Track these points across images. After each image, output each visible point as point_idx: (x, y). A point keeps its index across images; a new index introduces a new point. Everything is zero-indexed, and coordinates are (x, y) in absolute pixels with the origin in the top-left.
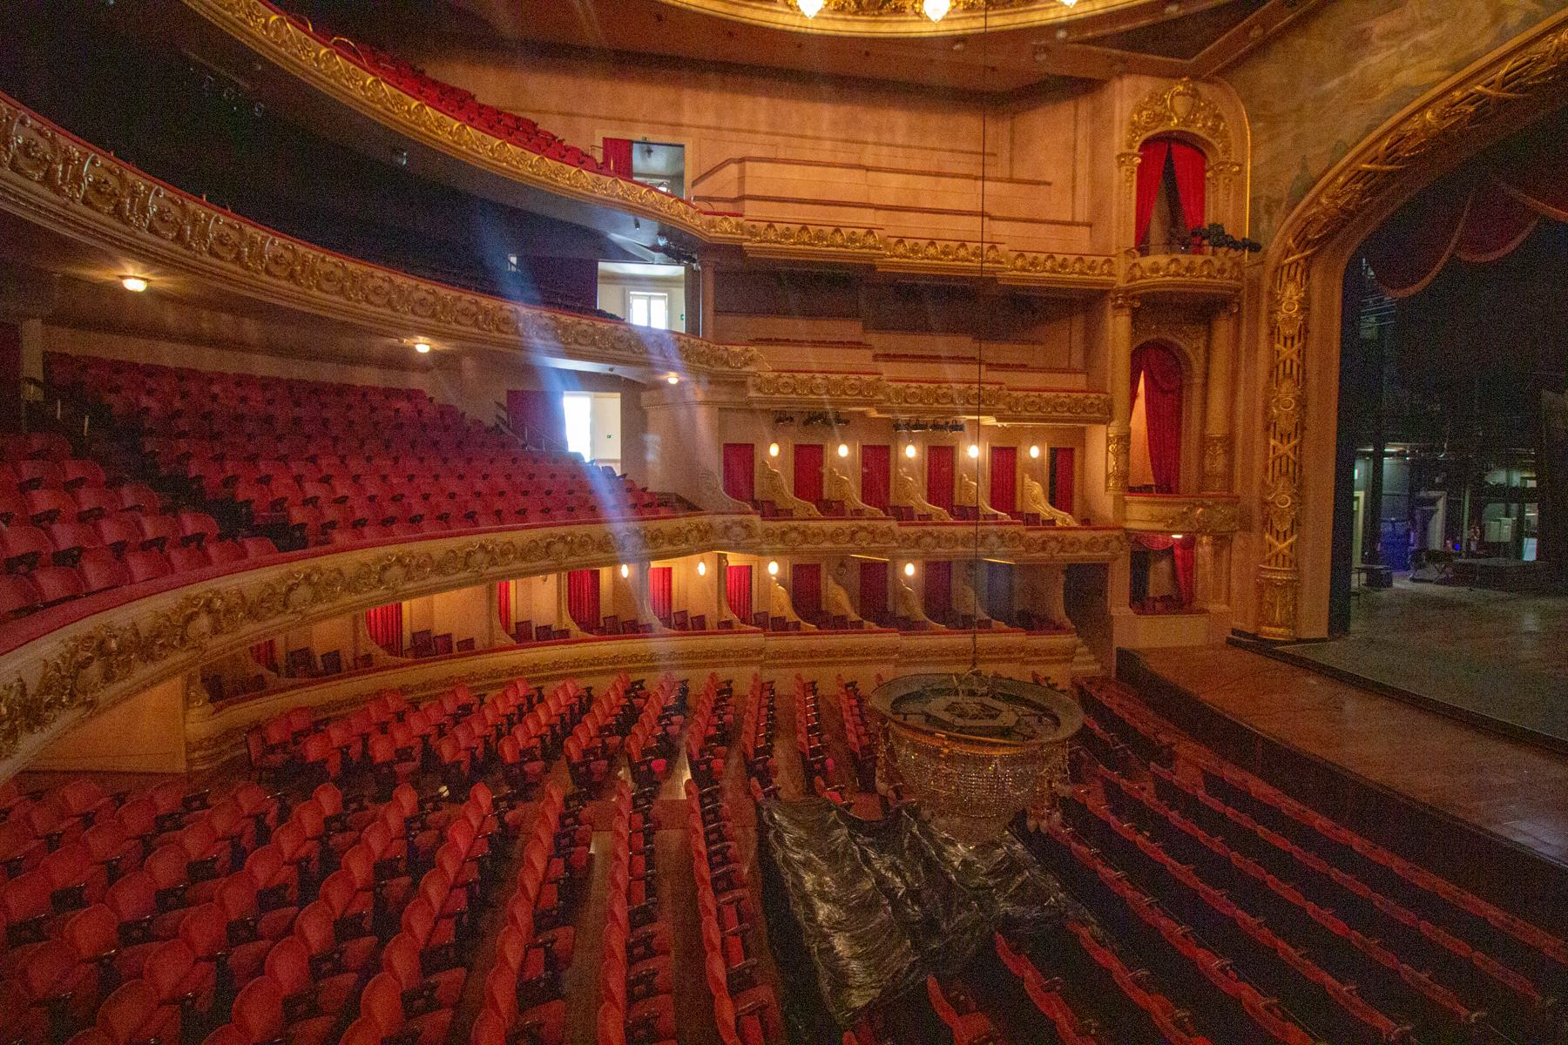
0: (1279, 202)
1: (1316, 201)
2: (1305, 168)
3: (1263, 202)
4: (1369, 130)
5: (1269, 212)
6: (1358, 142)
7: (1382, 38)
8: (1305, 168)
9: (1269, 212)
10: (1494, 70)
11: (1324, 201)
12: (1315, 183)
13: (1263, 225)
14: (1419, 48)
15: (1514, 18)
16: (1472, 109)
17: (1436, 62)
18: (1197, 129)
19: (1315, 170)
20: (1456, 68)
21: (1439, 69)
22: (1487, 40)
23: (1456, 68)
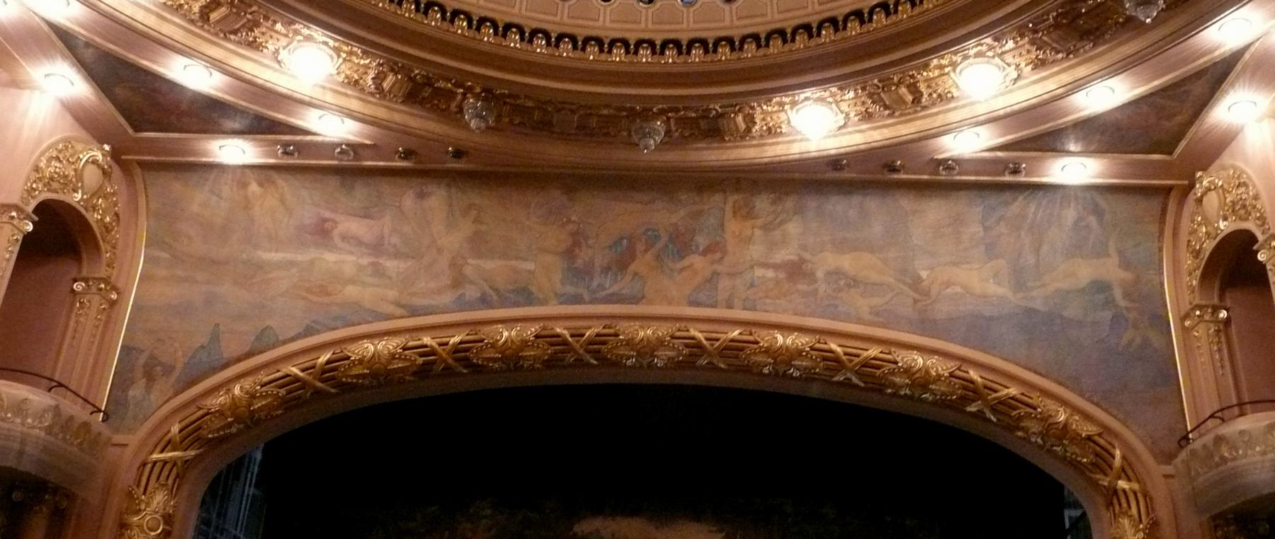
0: (168, 370)
2: (215, 338)
3: (142, 360)
4: (309, 332)
5: (150, 377)
6: (293, 339)
7: (344, 238)
9: (150, 377)
10: (450, 332)
11: (237, 391)
12: (226, 366)
13: (136, 392)
14: (378, 271)
15: (472, 293)
16: (421, 360)
17: (392, 294)
18: (93, 217)
19: (231, 348)
21: (398, 305)
22: (447, 298)
23: (414, 312)
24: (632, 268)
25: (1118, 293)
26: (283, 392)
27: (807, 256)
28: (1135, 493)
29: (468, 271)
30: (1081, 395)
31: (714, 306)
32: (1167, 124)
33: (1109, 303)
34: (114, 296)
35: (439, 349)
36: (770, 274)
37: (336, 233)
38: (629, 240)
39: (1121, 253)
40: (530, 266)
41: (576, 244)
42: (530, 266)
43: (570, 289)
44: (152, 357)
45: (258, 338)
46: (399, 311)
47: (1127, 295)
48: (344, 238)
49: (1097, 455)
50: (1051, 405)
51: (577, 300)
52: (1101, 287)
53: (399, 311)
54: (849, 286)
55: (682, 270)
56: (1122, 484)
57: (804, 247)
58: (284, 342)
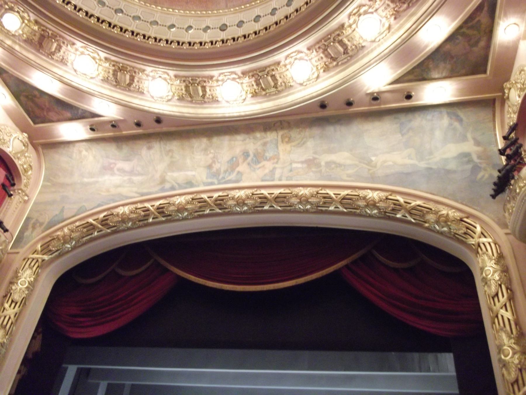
0: (41, 224)
1: (62, 228)
2: (62, 211)
3: (32, 221)
4: (99, 205)
8: (62, 211)
9: (34, 228)
14: (131, 182)
15: (167, 186)
16: (143, 213)
17: (135, 189)
18: (18, 163)
19: (67, 214)
20: (142, 195)
21: (136, 192)
23: (142, 195)
24: (238, 169)
25: (475, 157)
26: (85, 230)
27: (317, 156)
28: (489, 243)
29: (167, 178)
30: (456, 201)
31: (273, 180)
32: (475, 49)
33: (470, 161)
34: (26, 198)
35: (151, 208)
36: (299, 165)
37: (115, 169)
38: (236, 158)
39: (474, 139)
40: (193, 173)
41: (214, 162)
42: (193, 173)
43: (210, 180)
44: (37, 220)
45: (78, 210)
46: (136, 195)
47: (479, 157)
48: (119, 170)
49: (467, 228)
50: (441, 207)
51: (212, 184)
52: (465, 157)
53: (136, 195)
54: (337, 167)
55: (260, 168)
56: (483, 240)
57: (315, 153)
58: (89, 210)
